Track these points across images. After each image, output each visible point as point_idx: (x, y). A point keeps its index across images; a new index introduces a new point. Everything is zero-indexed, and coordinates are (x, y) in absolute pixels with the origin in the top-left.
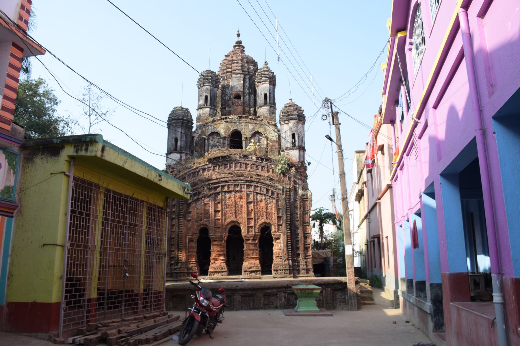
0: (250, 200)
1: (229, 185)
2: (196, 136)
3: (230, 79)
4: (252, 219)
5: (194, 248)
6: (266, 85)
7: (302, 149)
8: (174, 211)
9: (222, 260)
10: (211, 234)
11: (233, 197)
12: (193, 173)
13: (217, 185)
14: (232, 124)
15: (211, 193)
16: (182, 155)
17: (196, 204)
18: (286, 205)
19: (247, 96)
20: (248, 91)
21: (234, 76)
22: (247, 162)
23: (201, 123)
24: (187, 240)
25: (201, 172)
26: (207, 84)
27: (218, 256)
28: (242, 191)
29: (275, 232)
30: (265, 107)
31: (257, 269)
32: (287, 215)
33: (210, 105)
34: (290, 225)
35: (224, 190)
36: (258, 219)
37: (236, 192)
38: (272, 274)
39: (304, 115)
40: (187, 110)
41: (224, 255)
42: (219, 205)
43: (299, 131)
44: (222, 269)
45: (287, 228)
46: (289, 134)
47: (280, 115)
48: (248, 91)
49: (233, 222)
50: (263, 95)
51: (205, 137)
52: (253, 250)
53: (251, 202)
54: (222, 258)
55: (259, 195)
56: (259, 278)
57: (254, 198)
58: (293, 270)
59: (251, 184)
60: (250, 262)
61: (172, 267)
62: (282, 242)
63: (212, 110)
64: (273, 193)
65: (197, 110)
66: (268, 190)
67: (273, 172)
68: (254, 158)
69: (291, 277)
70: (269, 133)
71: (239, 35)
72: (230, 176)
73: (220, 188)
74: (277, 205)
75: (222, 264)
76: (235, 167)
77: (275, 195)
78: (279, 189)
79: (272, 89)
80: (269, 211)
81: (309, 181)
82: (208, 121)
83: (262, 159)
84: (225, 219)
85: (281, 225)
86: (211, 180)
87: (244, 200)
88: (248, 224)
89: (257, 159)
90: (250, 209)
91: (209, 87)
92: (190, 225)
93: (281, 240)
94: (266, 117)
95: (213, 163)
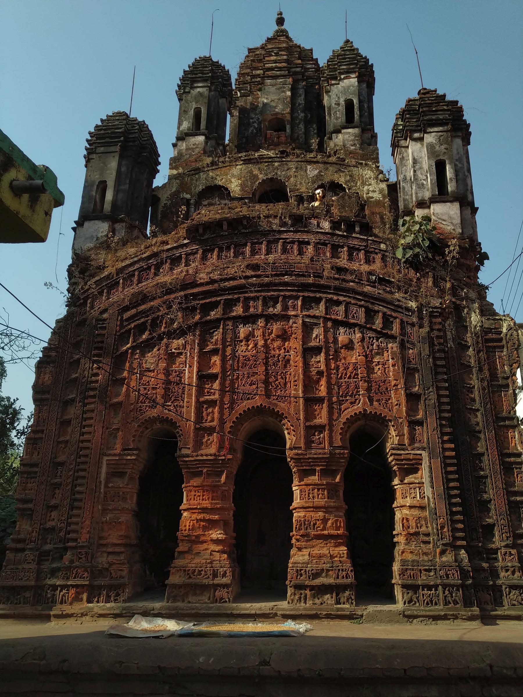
0: (313, 344)
1: (247, 300)
2: (164, 198)
3: (260, 90)
4: (321, 400)
5: (124, 499)
6: (352, 81)
7: (466, 202)
8: (76, 379)
9: (217, 542)
10: (185, 451)
11: (258, 333)
12: (141, 270)
13: (213, 299)
14: (264, 166)
15: (191, 322)
16: (118, 226)
17: (143, 355)
18: (434, 358)
19: (302, 126)
20: (302, 115)
21: (268, 82)
22: (305, 237)
23: (181, 170)
24: (104, 470)
25: (167, 266)
26: (200, 85)
27: (205, 529)
28: (287, 318)
29: (401, 446)
30: (350, 130)
31: (340, 581)
32: (438, 388)
33: (207, 128)
34: (451, 422)
35: (234, 314)
36: (340, 403)
37: (270, 318)
38: (391, 599)
39: (465, 121)
40: (143, 127)
41: (222, 524)
42: (216, 359)
43: (456, 157)
44: (215, 575)
45: (443, 434)
46: (426, 163)
47: (396, 125)
48: (302, 115)
49: (259, 411)
50: (342, 101)
51: (188, 196)
52: (326, 509)
53: (317, 350)
54: (217, 534)
55: (342, 330)
56: (351, 617)
57: (325, 337)
58: (475, 585)
59: (318, 295)
60: (316, 551)
61: (46, 566)
62: (426, 480)
63: (211, 143)
64: (387, 322)
65: (174, 145)
66: (370, 314)
67: (384, 259)
68: (326, 225)
69: (471, 618)
70: (363, 184)
71: (280, 21)
72: (250, 273)
73: (220, 309)
74: (405, 360)
75: (217, 556)
76: (268, 252)
77: (396, 329)
78: (408, 309)
79: (365, 92)
80: (381, 372)
81: (490, 298)
82: (199, 165)
83: (350, 227)
84: (233, 402)
85: (420, 423)
86: (194, 284)
87: (295, 344)
88: (307, 419)
89: (335, 225)
90: (314, 371)
91: (204, 91)
92: (116, 421)
93: (424, 473)
94: (351, 153)
95: (201, 242)
